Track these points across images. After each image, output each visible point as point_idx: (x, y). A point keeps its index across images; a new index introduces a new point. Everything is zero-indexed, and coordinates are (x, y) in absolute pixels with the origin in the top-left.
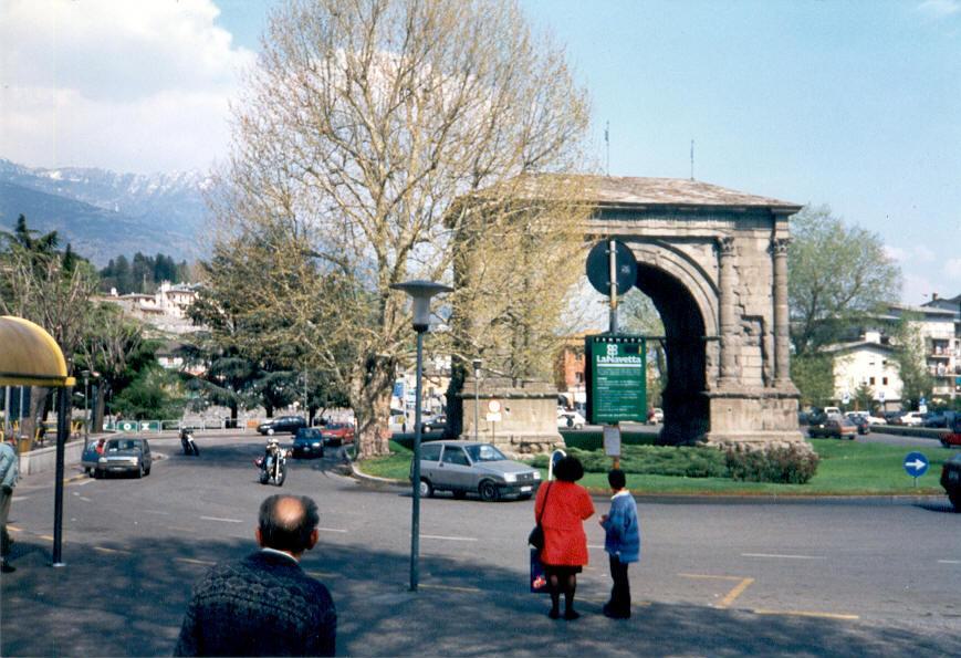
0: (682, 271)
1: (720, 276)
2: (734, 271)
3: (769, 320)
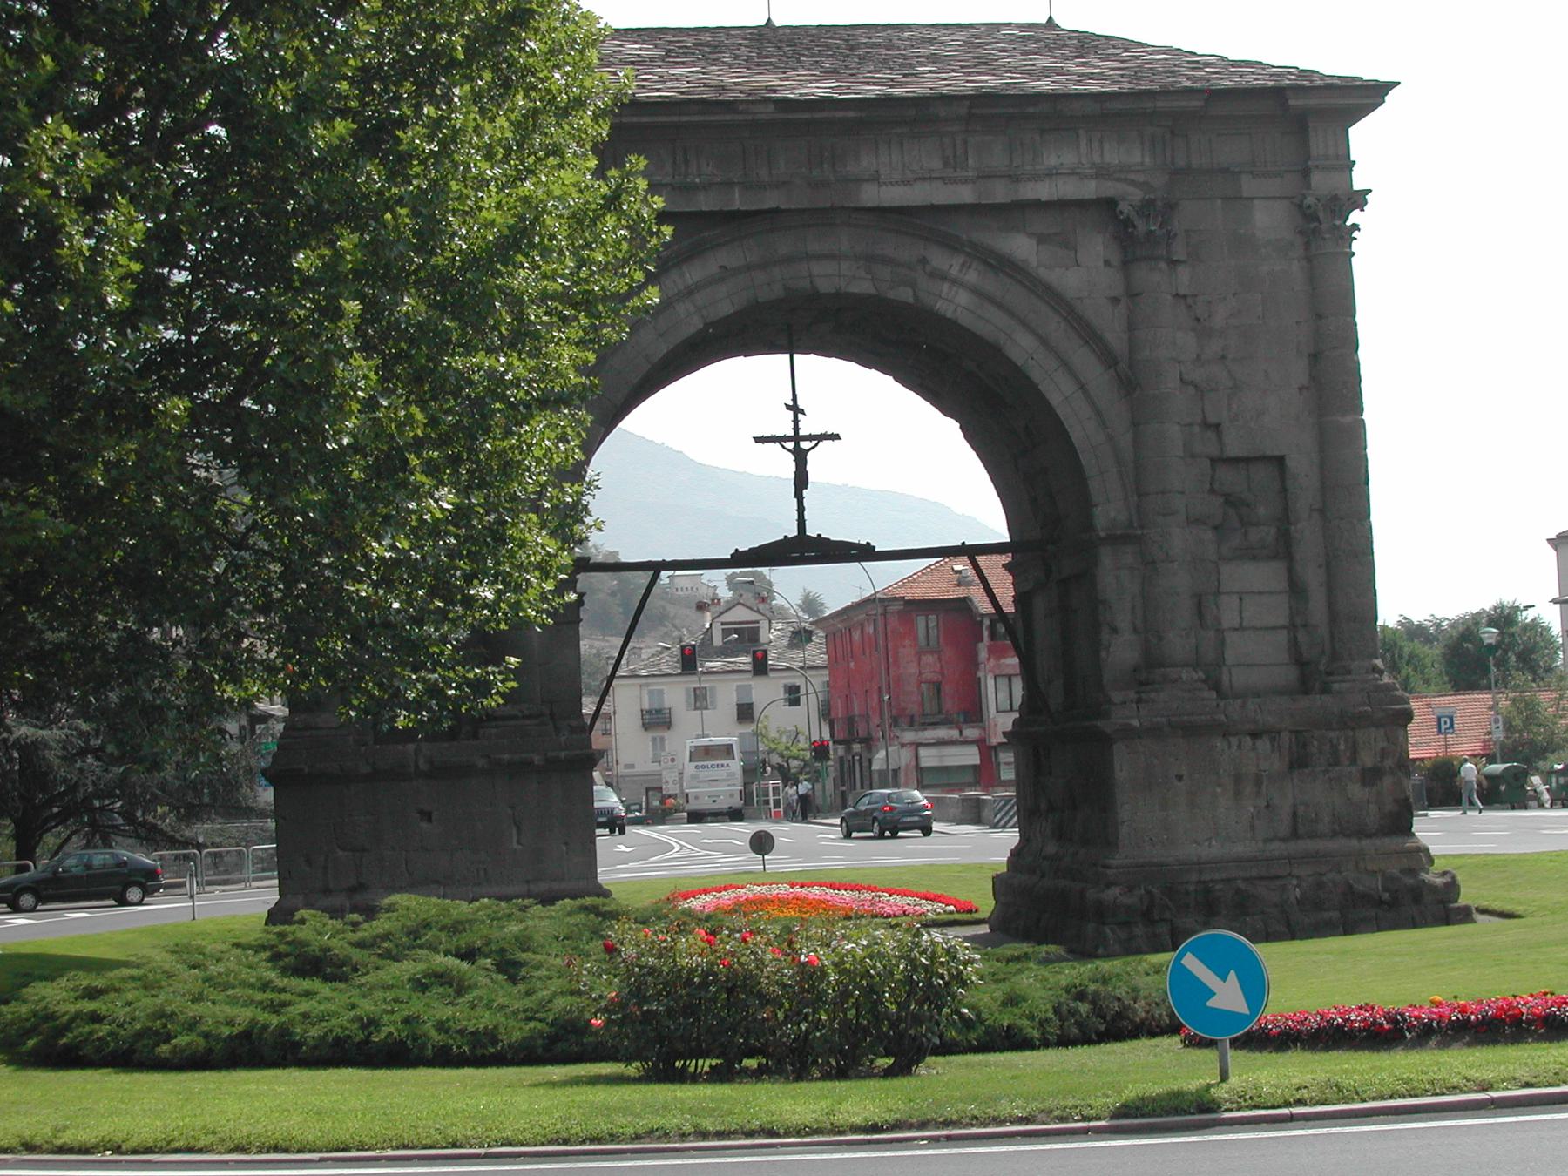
1: (1131, 327)
3: (1301, 464)
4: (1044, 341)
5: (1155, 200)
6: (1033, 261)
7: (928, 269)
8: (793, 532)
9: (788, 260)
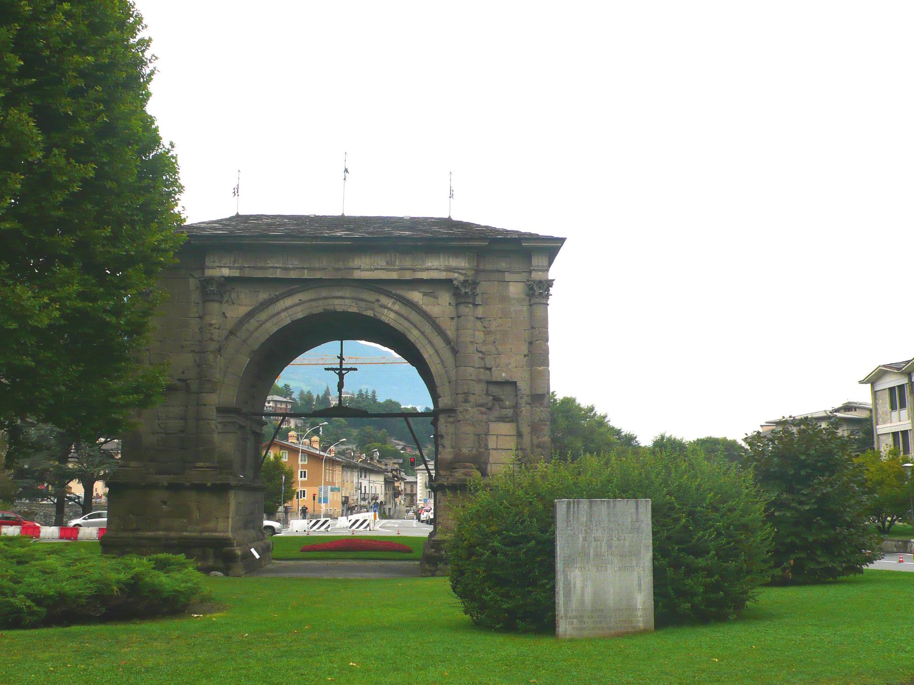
0: (407, 324)
1: (457, 330)
2: (479, 324)
3: (523, 386)
4: (423, 333)
5: (468, 280)
6: (421, 302)
7: (380, 303)
9: (326, 298)
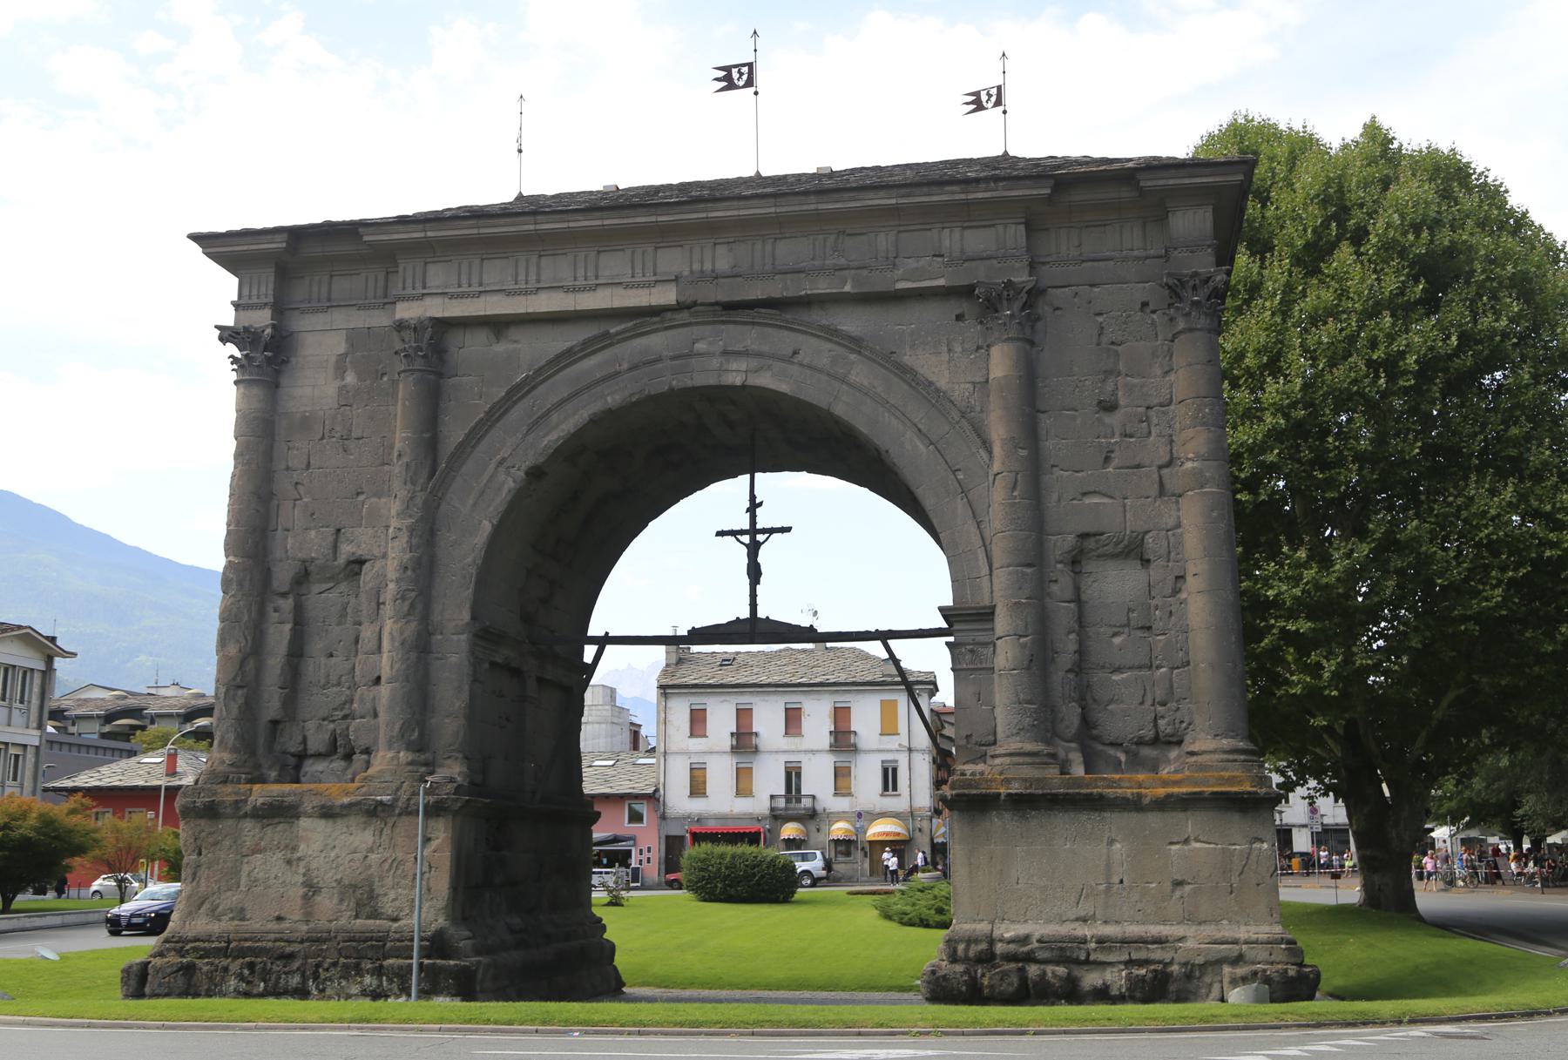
8: (745, 613)
